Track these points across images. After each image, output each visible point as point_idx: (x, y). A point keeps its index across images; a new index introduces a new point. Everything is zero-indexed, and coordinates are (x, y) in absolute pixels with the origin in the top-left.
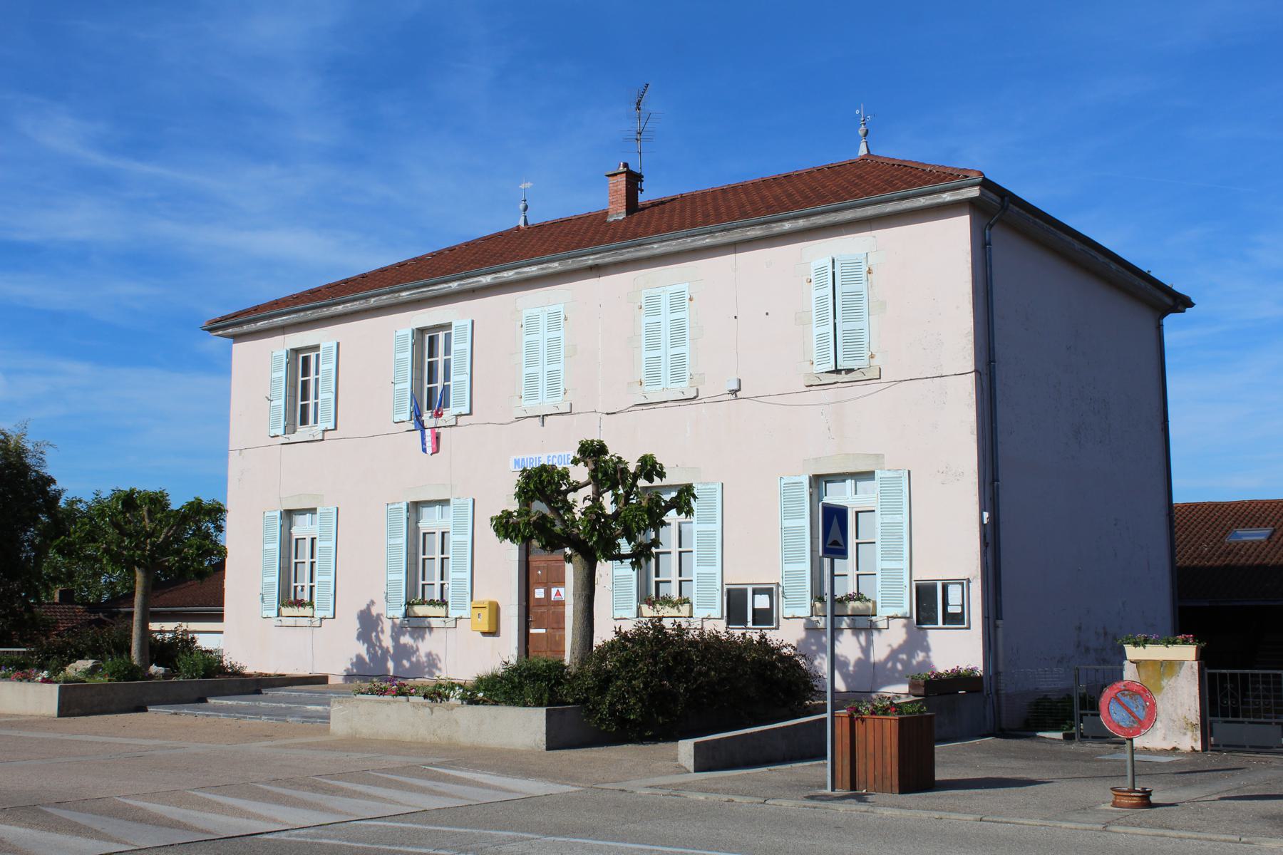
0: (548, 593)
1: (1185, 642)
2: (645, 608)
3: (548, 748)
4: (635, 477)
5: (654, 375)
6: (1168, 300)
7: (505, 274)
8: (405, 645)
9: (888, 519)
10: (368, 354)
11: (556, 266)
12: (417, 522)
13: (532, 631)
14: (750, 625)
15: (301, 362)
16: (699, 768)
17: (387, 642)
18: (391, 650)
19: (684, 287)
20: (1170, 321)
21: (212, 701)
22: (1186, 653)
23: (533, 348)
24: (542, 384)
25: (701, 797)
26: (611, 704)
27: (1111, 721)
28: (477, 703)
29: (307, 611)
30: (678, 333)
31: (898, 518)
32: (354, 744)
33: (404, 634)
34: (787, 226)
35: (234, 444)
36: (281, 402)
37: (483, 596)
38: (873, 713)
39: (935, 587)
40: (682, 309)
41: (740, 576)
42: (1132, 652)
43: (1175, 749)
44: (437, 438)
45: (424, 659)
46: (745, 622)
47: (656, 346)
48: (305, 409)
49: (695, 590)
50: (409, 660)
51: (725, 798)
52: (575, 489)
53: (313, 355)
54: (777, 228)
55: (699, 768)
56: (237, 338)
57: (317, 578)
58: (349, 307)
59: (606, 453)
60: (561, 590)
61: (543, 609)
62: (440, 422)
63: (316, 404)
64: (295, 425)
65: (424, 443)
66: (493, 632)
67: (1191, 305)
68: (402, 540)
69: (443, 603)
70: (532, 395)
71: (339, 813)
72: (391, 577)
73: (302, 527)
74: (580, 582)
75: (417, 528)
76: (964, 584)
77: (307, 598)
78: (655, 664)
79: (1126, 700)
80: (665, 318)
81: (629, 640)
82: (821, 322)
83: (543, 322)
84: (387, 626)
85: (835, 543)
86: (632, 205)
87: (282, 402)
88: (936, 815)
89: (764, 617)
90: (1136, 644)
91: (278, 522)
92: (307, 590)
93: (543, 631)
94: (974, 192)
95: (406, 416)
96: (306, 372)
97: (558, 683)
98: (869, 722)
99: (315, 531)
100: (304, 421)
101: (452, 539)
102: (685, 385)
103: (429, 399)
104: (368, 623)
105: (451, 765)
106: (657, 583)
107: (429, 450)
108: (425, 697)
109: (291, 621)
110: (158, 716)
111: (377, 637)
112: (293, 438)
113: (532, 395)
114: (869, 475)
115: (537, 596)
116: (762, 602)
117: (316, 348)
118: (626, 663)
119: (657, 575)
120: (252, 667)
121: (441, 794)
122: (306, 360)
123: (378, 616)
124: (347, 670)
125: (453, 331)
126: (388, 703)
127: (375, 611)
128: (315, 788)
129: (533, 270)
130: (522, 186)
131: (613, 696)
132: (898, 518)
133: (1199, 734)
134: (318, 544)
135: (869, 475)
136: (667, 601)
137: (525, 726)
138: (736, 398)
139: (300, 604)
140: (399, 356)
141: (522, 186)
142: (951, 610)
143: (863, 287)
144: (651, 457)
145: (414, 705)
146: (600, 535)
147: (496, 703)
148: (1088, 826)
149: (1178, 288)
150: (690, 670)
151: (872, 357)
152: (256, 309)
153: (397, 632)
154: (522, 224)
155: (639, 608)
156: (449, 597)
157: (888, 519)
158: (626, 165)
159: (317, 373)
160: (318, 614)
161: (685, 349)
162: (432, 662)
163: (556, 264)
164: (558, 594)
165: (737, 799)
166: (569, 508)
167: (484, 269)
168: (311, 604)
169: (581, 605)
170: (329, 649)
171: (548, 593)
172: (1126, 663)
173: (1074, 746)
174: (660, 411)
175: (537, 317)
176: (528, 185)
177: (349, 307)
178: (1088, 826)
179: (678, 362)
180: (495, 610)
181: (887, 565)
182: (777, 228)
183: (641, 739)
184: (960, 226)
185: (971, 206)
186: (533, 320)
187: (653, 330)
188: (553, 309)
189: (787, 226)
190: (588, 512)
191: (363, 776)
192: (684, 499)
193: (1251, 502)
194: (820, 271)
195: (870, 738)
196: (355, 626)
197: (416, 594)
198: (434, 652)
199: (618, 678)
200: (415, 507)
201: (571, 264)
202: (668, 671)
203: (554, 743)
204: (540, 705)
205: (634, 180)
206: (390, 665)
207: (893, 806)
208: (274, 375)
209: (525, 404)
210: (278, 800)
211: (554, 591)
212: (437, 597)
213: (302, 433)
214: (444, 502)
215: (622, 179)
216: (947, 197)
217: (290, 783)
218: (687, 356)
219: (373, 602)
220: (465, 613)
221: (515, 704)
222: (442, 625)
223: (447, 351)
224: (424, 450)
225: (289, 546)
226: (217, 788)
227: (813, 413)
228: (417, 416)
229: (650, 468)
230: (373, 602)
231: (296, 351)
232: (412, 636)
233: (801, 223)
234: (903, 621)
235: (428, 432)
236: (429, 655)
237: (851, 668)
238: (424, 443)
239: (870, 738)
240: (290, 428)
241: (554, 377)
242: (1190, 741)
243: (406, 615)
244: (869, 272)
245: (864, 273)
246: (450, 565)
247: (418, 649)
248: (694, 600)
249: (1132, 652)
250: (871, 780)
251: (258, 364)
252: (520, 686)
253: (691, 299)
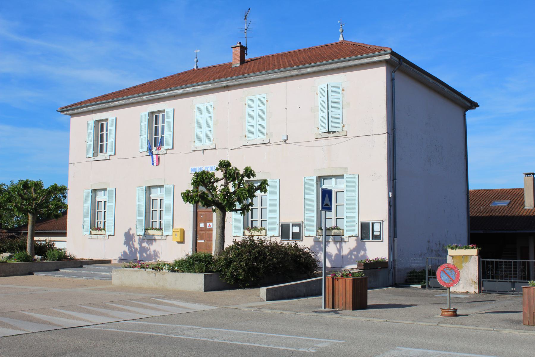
0: (205, 225)
1: (473, 248)
2: (246, 232)
3: (205, 291)
4: (243, 176)
5: (251, 133)
6: (469, 104)
7: (188, 89)
8: (144, 247)
9: (349, 195)
10: (129, 123)
11: (210, 86)
12: (150, 195)
13: (198, 241)
14: (291, 239)
15: (100, 126)
16: (268, 299)
17: (137, 246)
18: (139, 249)
19: (265, 95)
20: (469, 113)
21: (61, 270)
22: (473, 252)
23: (200, 121)
24: (204, 136)
25: (269, 311)
26: (232, 272)
27: (441, 280)
28: (175, 271)
29: (102, 232)
30: (261, 115)
31: (353, 195)
32: (122, 289)
33: (144, 242)
34: (308, 70)
35: (71, 160)
36: (91, 143)
37: (178, 226)
38: (342, 277)
39: (369, 224)
40: (263, 105)
41: (286, 219)
42: (450, 252)
43: (467, 292)
44: (158, 159)
45: (152, 253)
46: (289, 238)
47: (252, 121)
48: (102, 146)
49: (268, 224)
50: (146, 253)
51: (280, 312)
52: (217, 181)
53: (105, 123)
54: (304, 71)
55: (268, 299)
56: (72, 115)
57: (107, 218)
58: (121, 102)
59: (230, 166)
60: (211, 224)
61: (203, 232)
62: (160, 152)
63: (107, 144)
64: (97, 153)
65: (153, 161)
66: (182, 242)
67: (478, 106)
68: (143, 202)
69: (161, 229)
70: (199, 141)
71: (116, 318)
72: (139, 218)
73: (101, 197)
74: (219, 221)
75: (150, 197)
76: (381, 222)
77: (102, 227)
78: (251, 255)
79: (447, 271)
80: (256, 109)
81: (239, 245)
82: (322, 111)
83: (204, 110)
84: (137, 238)
85: (327, 205)
86: (243, 61)
87: (92, 143)
88: (368, 319)
89: (296, 236)
90: (452, 248)
91: (90, 194)
92: (102, 223)
93: (203, 241)
94: (388, 57)
95: (145, 150)
96: (102, 130)
97: (209, 263)
98: (340, 280)
99: (106, 198)
100: (101, 151)
101: (164, 202)
102: (264, 137)
103: (155, 142)
104: (129, 237)
105: (164, 298)
106: (252, 221)
107: (155, 164)
108: (153, 269)
109: (95, 237)
110: (38, 276)
111: (133, 243)
112: (97, 158)
113: (199, 141)
114: (342, 176)
116: (296, 230)
117: (107, 120)
118: (238, 255)
119: (252, 218)
120: (79, 256)
121: (159, 310)
122: (102, 125)
123: (133, 234)
124: (120, 257)
125: (165, 113)
126: (137, 271)
127: (131, 232)
128: (105, 307)
129: (200, 88)
130: (196, 52)
131: (233, 269)
132: (353, 195)
133: (477, 286)
134: (107, 204)
135: (342, 176)
136: (256, 229)
137: (195, 281)
138: (286, 143)
139: (99, 229)
140: (142, 124)
141: (196, 52)
142: (375, 233)
143: (340, 97)
144: (250, 168)
145: (148, 272)
146: (227, 201)
147: (183, 272)
148: (431, 324)
149: (473, 99)
150: (265, 258)
151: (344, 126)
152: (81, 103)
153: (141, 241)
154: (195, 68)
155: (244, 232)
156: (163, 227)
157: (349, 195)
158: (240, 43)
159: (107, 131)
160: (107, 234)
161: (265, 122)
162: (156, 254)
163: (210, 85)
164: (210, 225)
165: (284, 312)
166: (215, 189)
167: (179, 87)
168: (104, 229)
169: (219, 230)
170: (111, 248)
171: (205, 225)
172: (448, 256)
173: (426, 291)
174: (253, 148)
175: (201, 108)
176: (198, 51)
177: (121, 102)
178: (431, 324)
179: (261, 127)
180: (183, 232)
181: (349, 214)
182: (304, 71)
183: (244, 287)
184: (381, 72)
185: (387, 62)
186: (200, 110)
187: (251, 114)
188: (208, 104)
189: (308, 70)
190: (222, 191)
191: (126, 302)
192: (263, 186)
193: (501, 190)
194: (322, 89)
195: (341, 287)
196: (123, 239)
197: (149, 226)
198: (157, 250)
199: (234, 261)
200: (149, 188)
201: (216, 85)
202: (256, 258)
203: (207, 289)
204: (202, 272)
205: (243, 50)
206: (138, 255)
207: (350, 315)
208: (89, 131)
209: (196, 145)
210: (90, 312)
211: (208, 224)
212: (158, 227)
213: (101, 156)
214: (161, 186)
215: (238, 49)
216: (376, 59)
217: (95, 305)
218: (265, 125)
219: (131, 229)
220: (170, 233)
221: (191, 272)
222: (160, 238)
223: (163, 122)
224: (153, 164)
225: (95, 205)
226: (63, 307)
227: (319, 150)
228: (150, 149)
229: (249, 172)
230: (131, 229)
231: (98, 121)
232: (147, 243)
233: (314, 69)
234: (355, 238)
235: (155, 156)
236: (155, 251)
237: (333, 258)
238: (153, 161)
239: (341, 287)
240: (95, 154)
241: (208, 133)
242: (474, 289)
243: (145, 234)
244: (343, 90)
245: (341, 91)
246: (163, 213)
247: (150, 249)
248: (267, 229)
249: (450, 252)
250: (340, 305)
251: (82, 126)
252: (193, 264)
253: (267, 101)
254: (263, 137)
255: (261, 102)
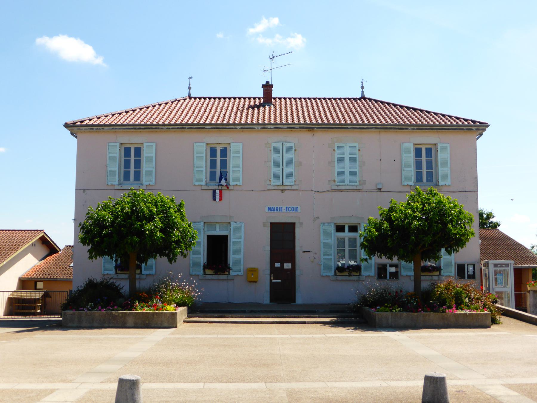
30: (353, 163)
39: (464, 265)
46: (465, 278)
80: (347, 156)
89: (395, 275)
93: (280, 281)
115: (276, 266)
116: (393, 270)
155: (335, 272)
171: (282, 266)
179: (353, 176)
211: (285, 264)
224: (214, 199)
253: (359, 150)
254: (356, 184)
255: (352, 150)
